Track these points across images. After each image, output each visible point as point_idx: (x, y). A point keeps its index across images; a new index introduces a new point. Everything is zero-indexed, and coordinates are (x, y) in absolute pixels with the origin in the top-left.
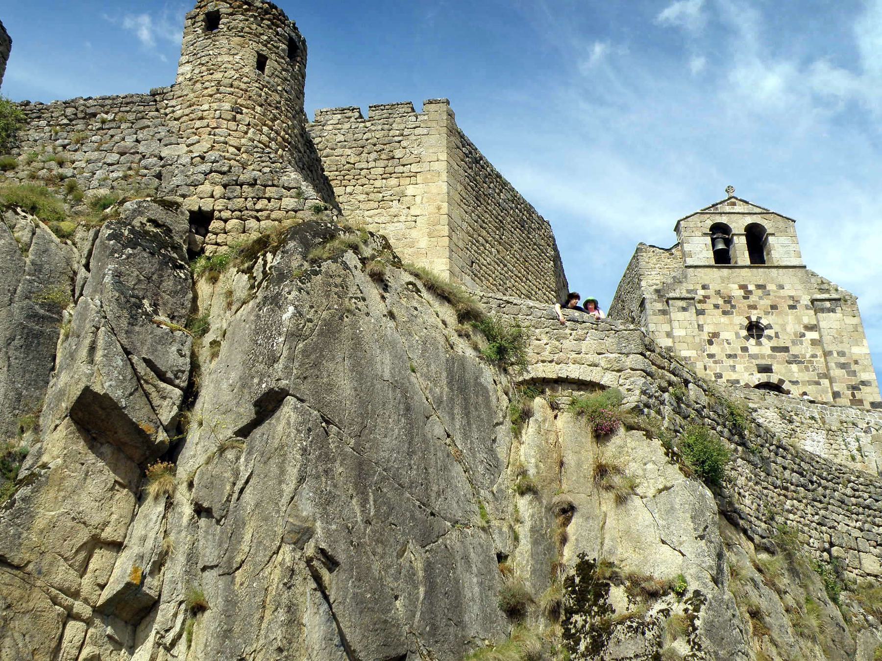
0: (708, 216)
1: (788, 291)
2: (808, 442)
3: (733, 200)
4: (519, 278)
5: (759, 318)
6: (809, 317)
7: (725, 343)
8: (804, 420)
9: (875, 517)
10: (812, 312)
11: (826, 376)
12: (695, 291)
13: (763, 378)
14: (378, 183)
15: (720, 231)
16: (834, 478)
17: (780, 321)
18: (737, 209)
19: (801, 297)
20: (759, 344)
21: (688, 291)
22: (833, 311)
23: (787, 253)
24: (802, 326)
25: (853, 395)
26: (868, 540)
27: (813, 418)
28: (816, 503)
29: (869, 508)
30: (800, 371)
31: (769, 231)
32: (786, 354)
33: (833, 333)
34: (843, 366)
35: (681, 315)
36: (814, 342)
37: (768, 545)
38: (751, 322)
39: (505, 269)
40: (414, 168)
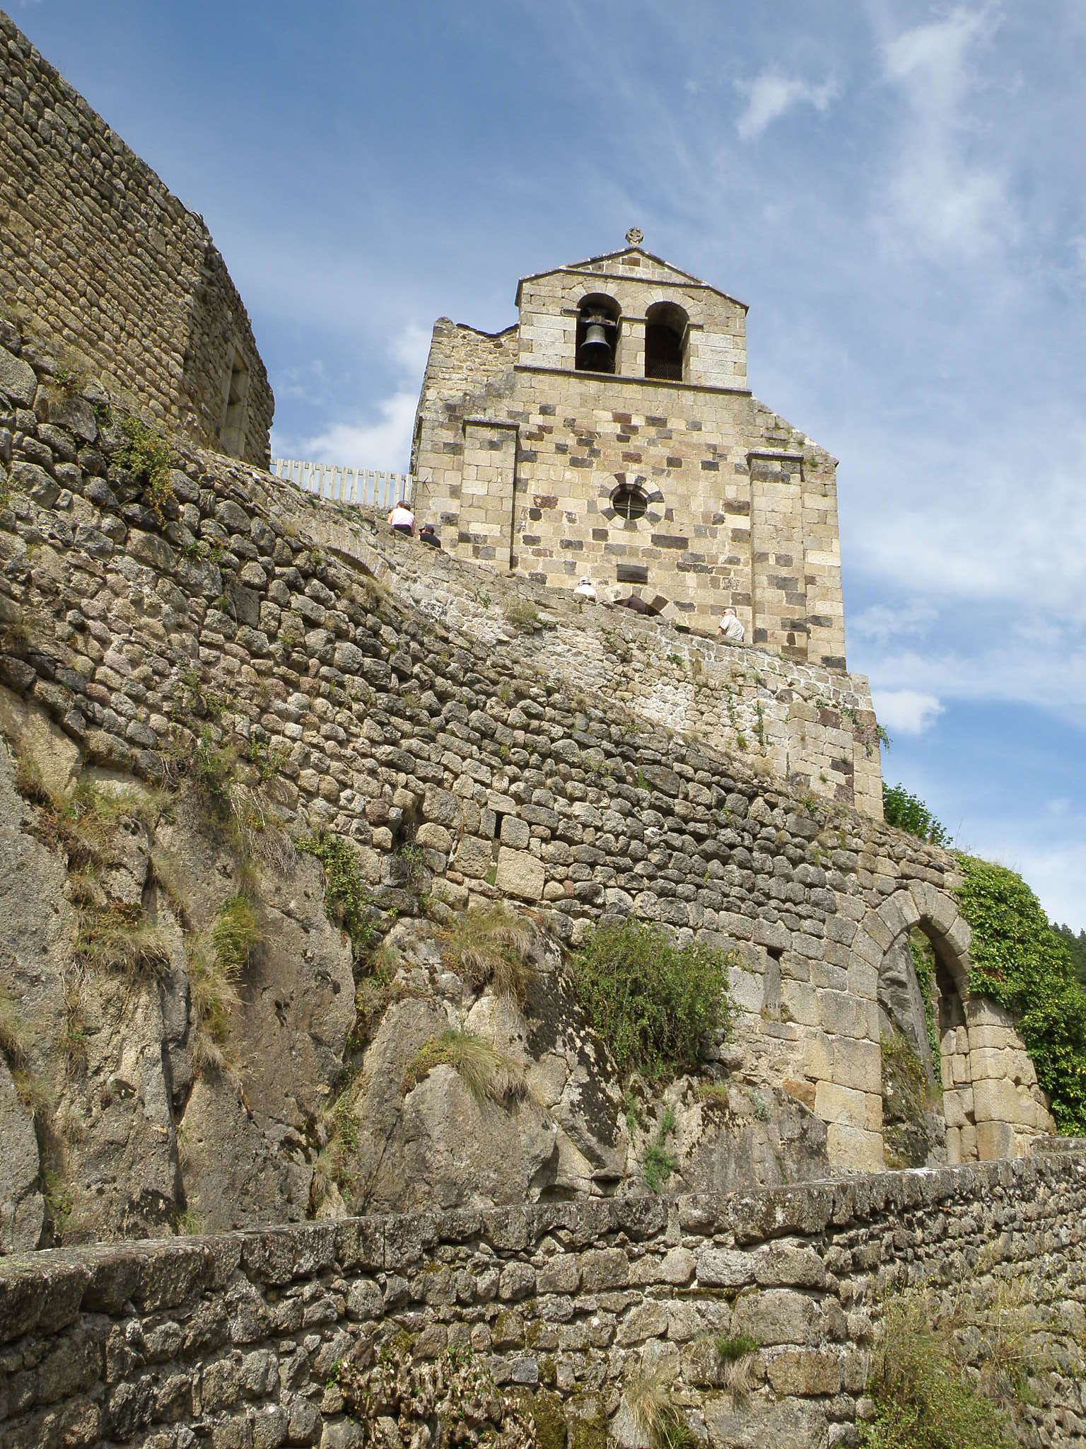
0: (581, 278)
1: (709, 436)
2: (654, 702)
3: (635, 255)
4: (65, 293)
6: (736, 488)
7: (565, 520)
8: (653, 660)
9: (567, 777)
10: (746, 479)
11: (748, 600)
13: (626, 590)
16: (479, 681)
17: (682, 490)
18: (639, 272)
19: (729, 448)
20: (631, 527)
21: (511, 414)
22: (785, 479)
23: (721, 364)
24: (721, 502)
25: (791, 639)
26: (530, 824)
27: (675, 659)
28: (393, 719)
29: (558, 758)
31: (692, 320)
32: (680, 552)
33: (777, 519)
34: (782, 583)
35: (484, 456)
36: (738, 536)
37: (144, 762)
38: (623, 486)
39: (20, 261)
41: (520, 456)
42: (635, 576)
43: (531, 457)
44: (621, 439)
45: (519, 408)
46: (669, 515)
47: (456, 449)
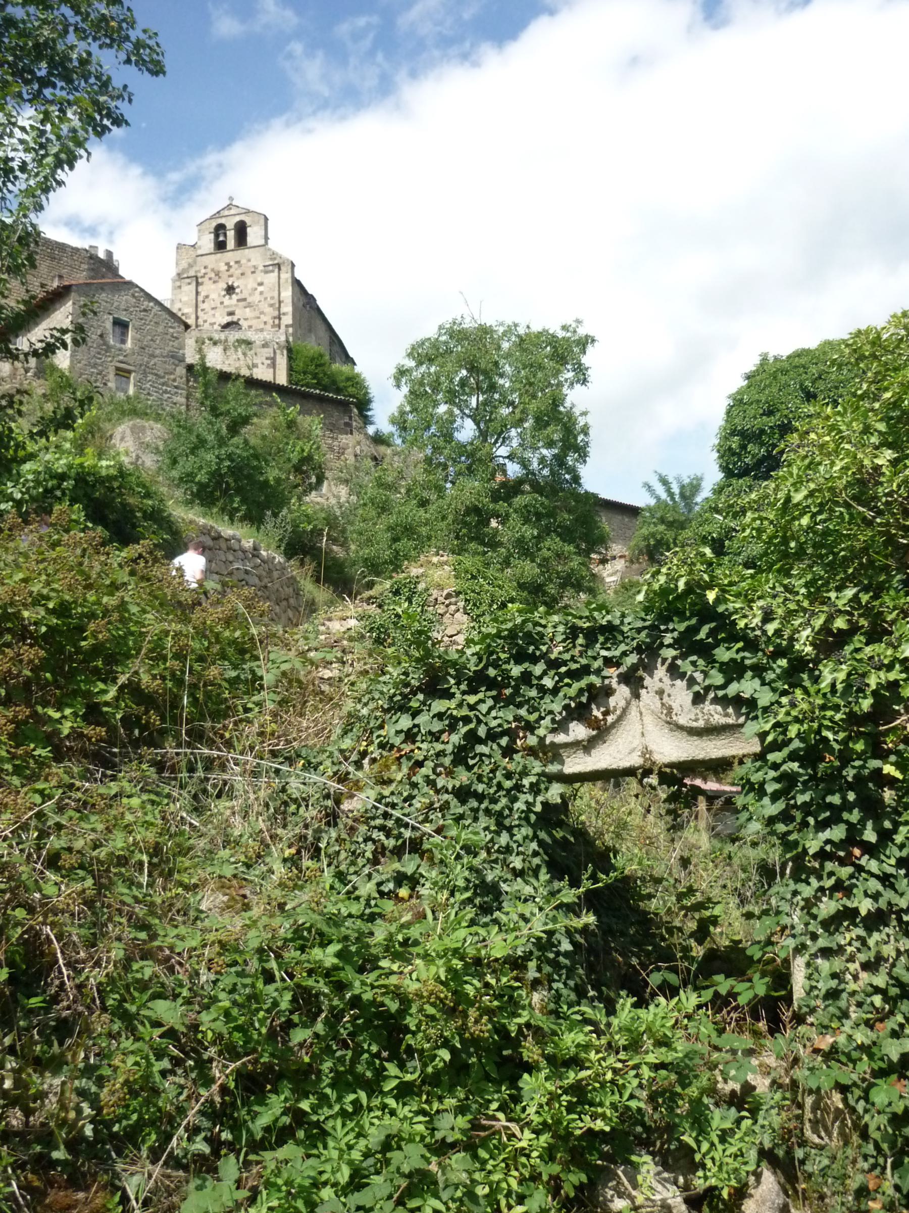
1: (253, 263)
12: (199, 271)
13: (229, 319)
15: (220, 229)
18: (232, 212)
22: (273, 271)
34: (271, 305)
36: (261, 293)
41: (198, 284)
42: (231, 314)
43: (202, 284)
47: (180, 287)
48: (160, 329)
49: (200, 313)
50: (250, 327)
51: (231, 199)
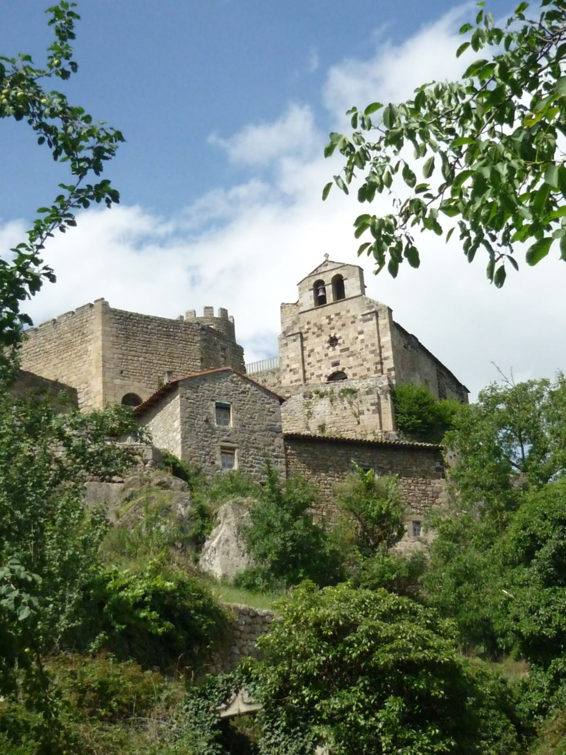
1: (352, 313)
2: (319, 406)
5: (335, 334)
12: (303, 327)
14: (79, 348)
15: (319, 285)
18: (329, 268)
20: (334, 350)
21: (300, 328)
22: (371, 319)
23: (353, 288)
30: (354, 360)
31: (344, 277)
34: (373, 352)
36: (362, 341)
38: (331, 338)
40: (90, 337)
41: (303, 340)
42: (336, 364)
43: (306, 339)
44: (329, 323)
45: (301, 325)
46: (344, 342)
47: (286, 344)
48: (258, 406)
49: (307, 367)
50: (355, 375)
51: (327, 255)
